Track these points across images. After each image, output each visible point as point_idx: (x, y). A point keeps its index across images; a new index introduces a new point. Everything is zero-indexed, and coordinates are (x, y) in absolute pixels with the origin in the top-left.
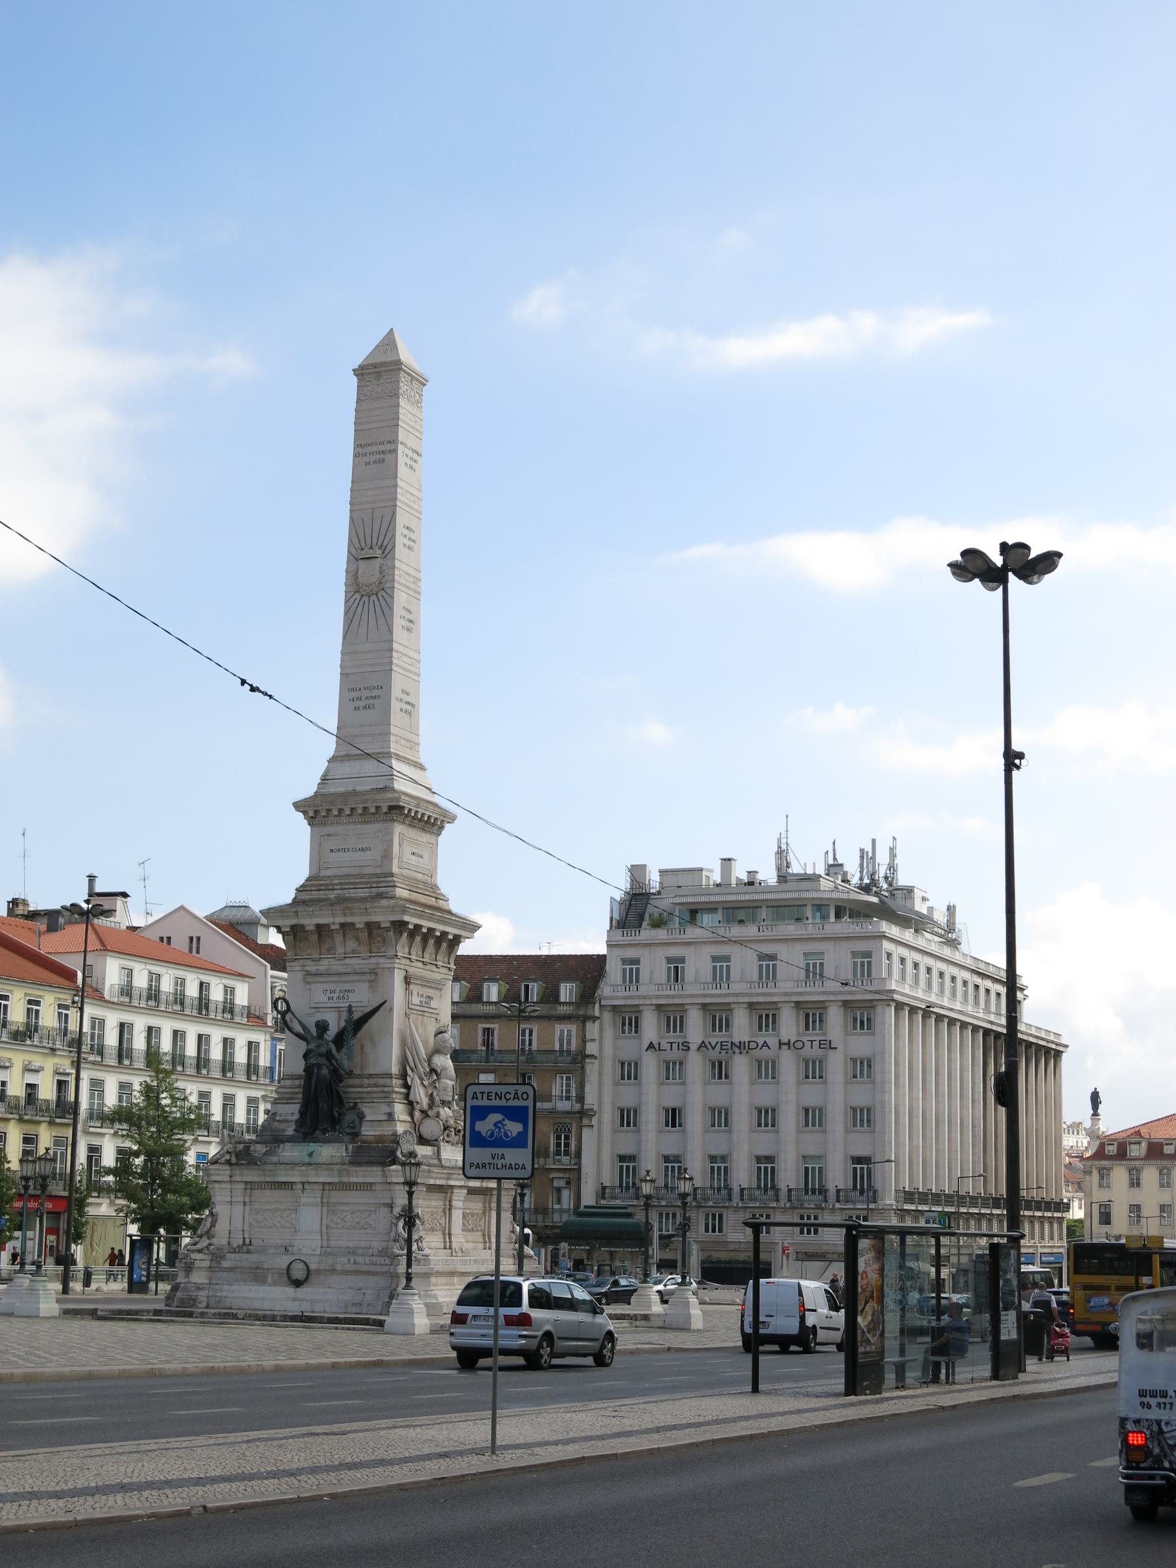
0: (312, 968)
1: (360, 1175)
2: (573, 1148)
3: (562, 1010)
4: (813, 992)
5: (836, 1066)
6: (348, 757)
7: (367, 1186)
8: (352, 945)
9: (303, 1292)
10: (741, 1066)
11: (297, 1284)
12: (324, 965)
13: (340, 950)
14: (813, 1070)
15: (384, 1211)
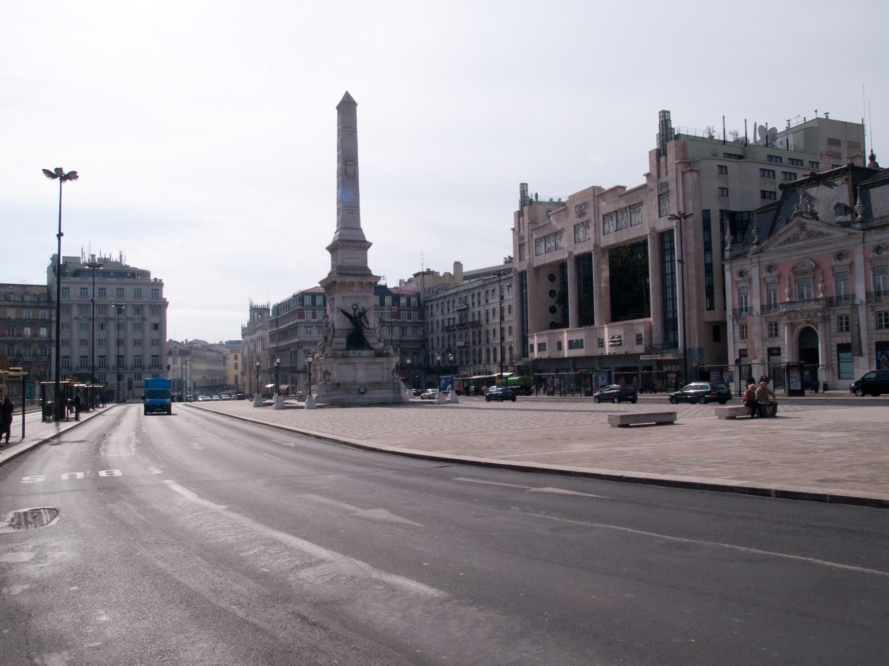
0: (344, 294)
1: (379, 360)
2: (48, 353)
3: (42, 304)
4: (138, 302)
5: (147, 326)
6: (346, 228)
7: (380, 363)
8: (359, 288)
9: (365, 396)
10: (112, 326)
11: (363, 393)
12: (349, 294)
13: (355, 290)
14: (138, 326)
15: (386, 371)
